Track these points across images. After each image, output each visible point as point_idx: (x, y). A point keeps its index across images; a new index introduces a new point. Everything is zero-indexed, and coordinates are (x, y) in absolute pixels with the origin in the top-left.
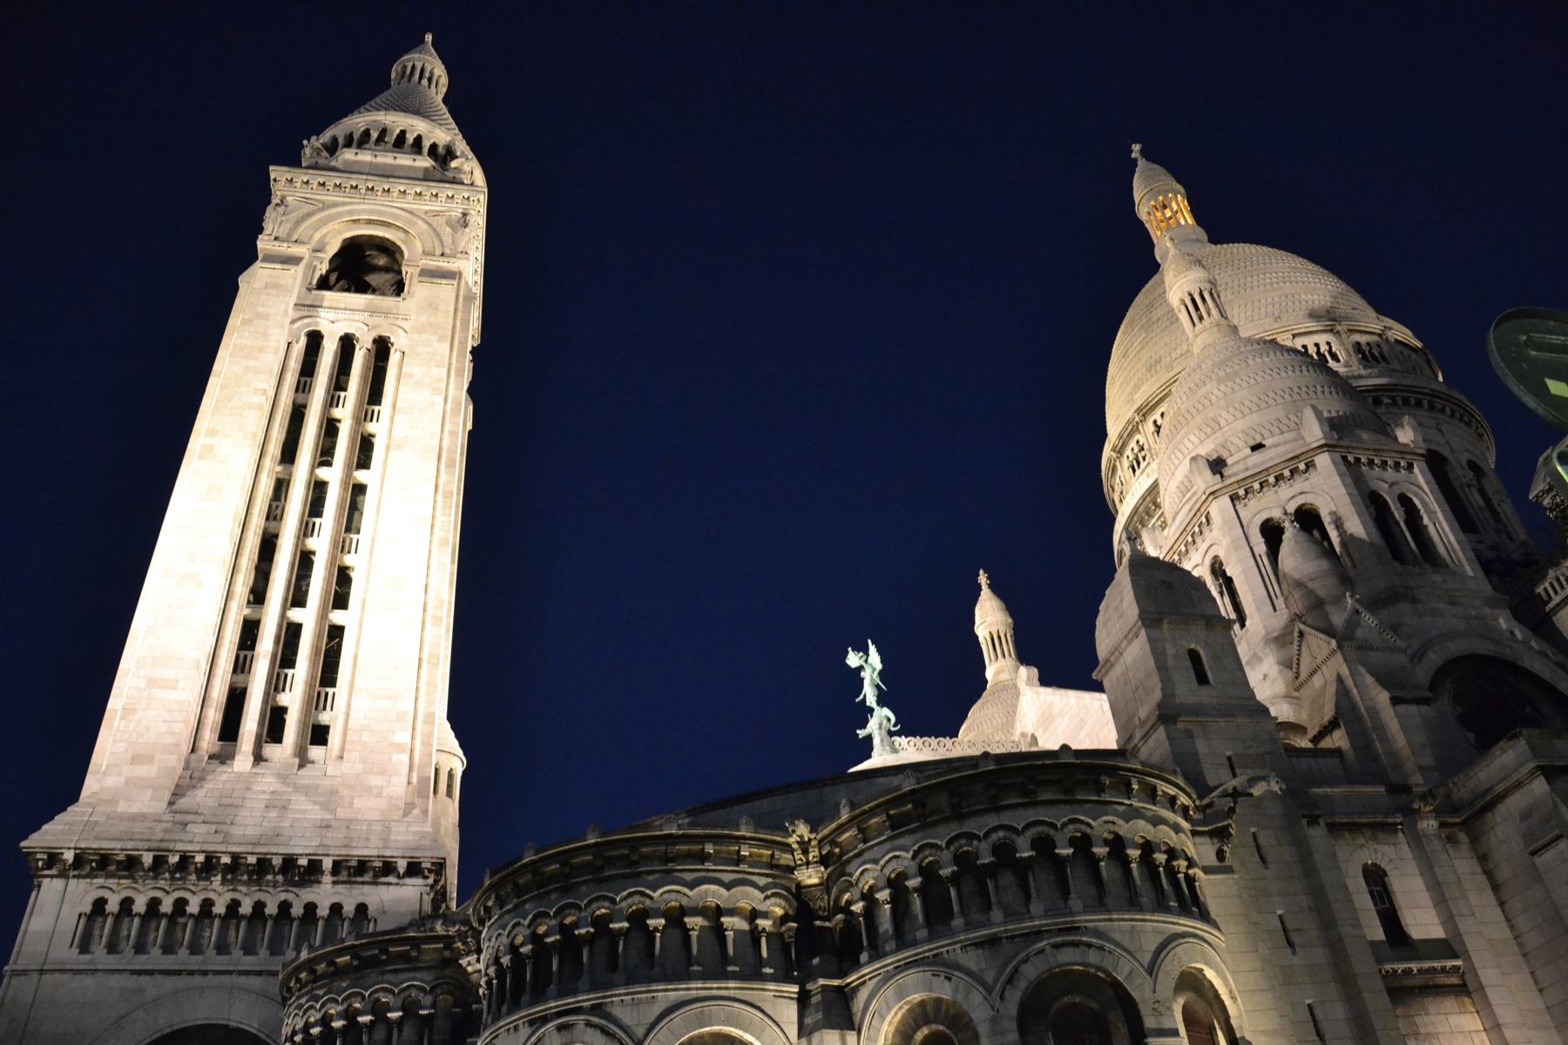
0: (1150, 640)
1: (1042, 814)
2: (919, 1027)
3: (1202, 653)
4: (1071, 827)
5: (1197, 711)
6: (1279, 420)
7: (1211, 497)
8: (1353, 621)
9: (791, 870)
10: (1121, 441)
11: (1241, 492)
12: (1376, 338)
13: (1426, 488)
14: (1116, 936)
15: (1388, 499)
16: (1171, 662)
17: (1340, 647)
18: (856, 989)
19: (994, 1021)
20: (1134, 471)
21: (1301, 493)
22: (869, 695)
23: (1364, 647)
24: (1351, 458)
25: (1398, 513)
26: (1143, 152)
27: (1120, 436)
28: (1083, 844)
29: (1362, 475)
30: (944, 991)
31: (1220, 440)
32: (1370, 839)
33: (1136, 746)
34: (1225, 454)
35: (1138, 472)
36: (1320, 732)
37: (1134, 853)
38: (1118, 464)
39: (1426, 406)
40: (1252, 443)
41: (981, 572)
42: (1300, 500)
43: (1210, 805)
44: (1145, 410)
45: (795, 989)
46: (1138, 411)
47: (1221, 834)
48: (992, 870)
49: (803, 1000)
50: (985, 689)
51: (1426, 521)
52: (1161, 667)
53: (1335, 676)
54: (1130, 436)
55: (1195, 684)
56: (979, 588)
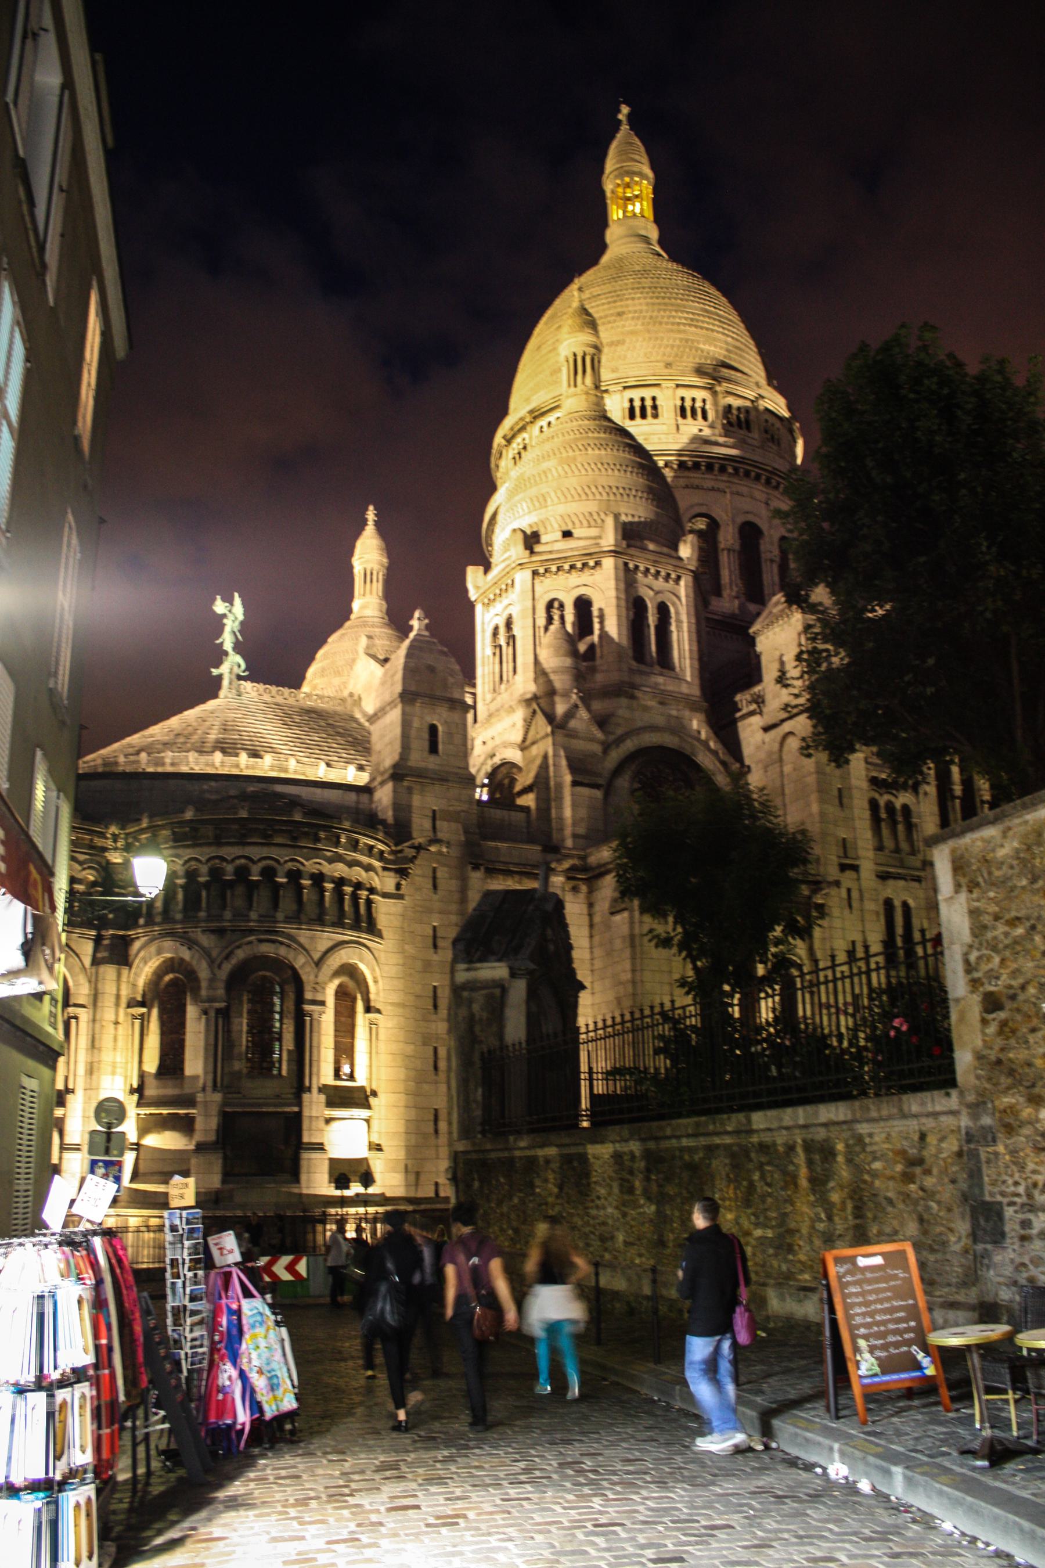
0: (404, 713)
1: (273, 852)
2: (167, 973)
3: (440, 728)
4: (290, 864)
5: (420, 774)
6: (590, 514)
8: (570, 714)
9: (105, 849)
11: (541, 570)
12: (748, 404)
13: (684, 599)
14: (302, 940)
15: (649, 605)
16: (413, 733)
17: (553, 733)
18: (133, 940)
19: (212, 980)
22: (227, 641)
23: (573, 735)
24: (631, 566)
25: (652, 619)
26: (630, 117)
27: (512, 429)
28: (295, 876)
29: (635, 581)
30: (186, 954)
34: (542, 531)
37: (329, 886)
40: (565, 528)
41: (371, 508)
43: (401, 851)
45: (94, 933)
46: (531, 412)
47: (403, 873)
48: (231, 884)
49: (98, 941)
50: (348, 619)
51: (673, 628)
52: (405, 736)
53: (542, 753)
55: (426, 754)
56: (364, 523)
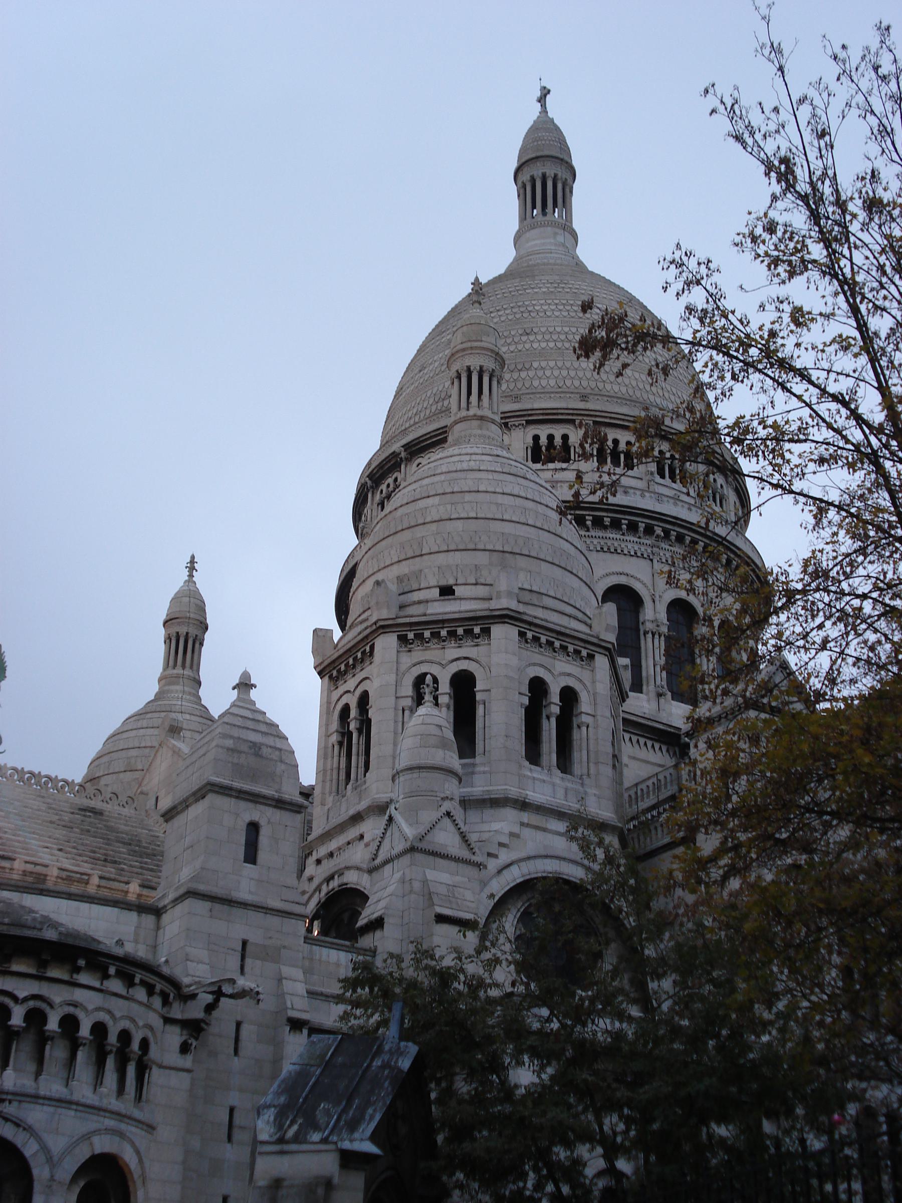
24: (530, 635)
27: (381, 466)
33: (165, 906)
38: (370, 495)
40: (443, 583)
42: (463, 665)
46: (406, 447)
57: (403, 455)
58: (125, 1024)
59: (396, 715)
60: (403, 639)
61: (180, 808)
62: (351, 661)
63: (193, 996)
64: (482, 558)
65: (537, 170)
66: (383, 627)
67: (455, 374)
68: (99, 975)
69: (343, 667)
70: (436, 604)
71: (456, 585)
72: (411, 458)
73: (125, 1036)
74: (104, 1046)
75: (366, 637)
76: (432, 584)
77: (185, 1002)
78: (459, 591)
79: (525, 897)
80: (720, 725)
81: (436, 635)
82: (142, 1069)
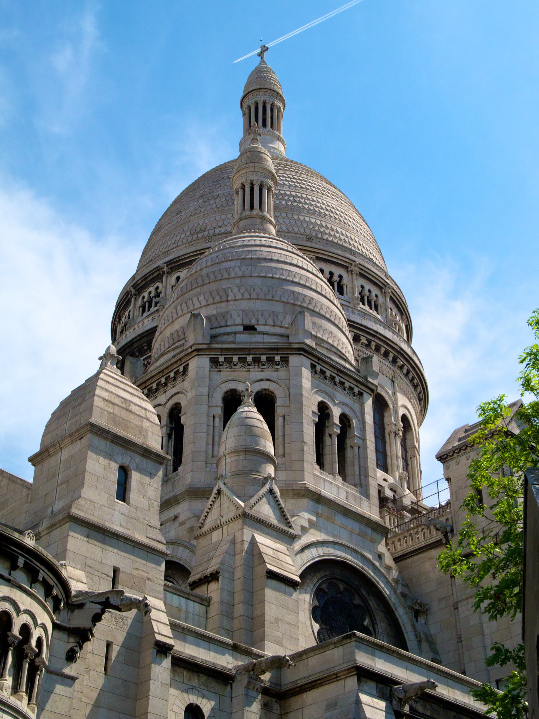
7: (196, 353)
10: (144, 282)
20: (144, 311)
21: (268, 380)
24: (318, 368)
27: (145, 277)
31: (224, 310)
32: (203, 684)
35: (145, 314)
36: (200, 580)
38: (133, 300)
39: (391, 358)
40: (247, 322)
42: (265, 385)
44: (174, 265)
46: (168, 263)
54: (153, 281)
57: (165, 269)
58: (25, 619)
59: (208, 420)
60: (214, 362)
61: (51, 450)
62: (163, 380)
63: (81, 606)
64: (278, 308)
65: (260, 98)
66: (197, 350)
67: (240, 186)
68: (8, 564)
69: (154, 386)
70: (242, 336)
71: (258, 324)
72: (171, 272)
73: (25, 630)
74: (8, 636)
75: (180, 359)
76: (237, 323)
77: (72, 612)
78: (259, 328)
79: (319, 575)
80: (472, 450)
81: (242, 360)
82: (34, 670)
